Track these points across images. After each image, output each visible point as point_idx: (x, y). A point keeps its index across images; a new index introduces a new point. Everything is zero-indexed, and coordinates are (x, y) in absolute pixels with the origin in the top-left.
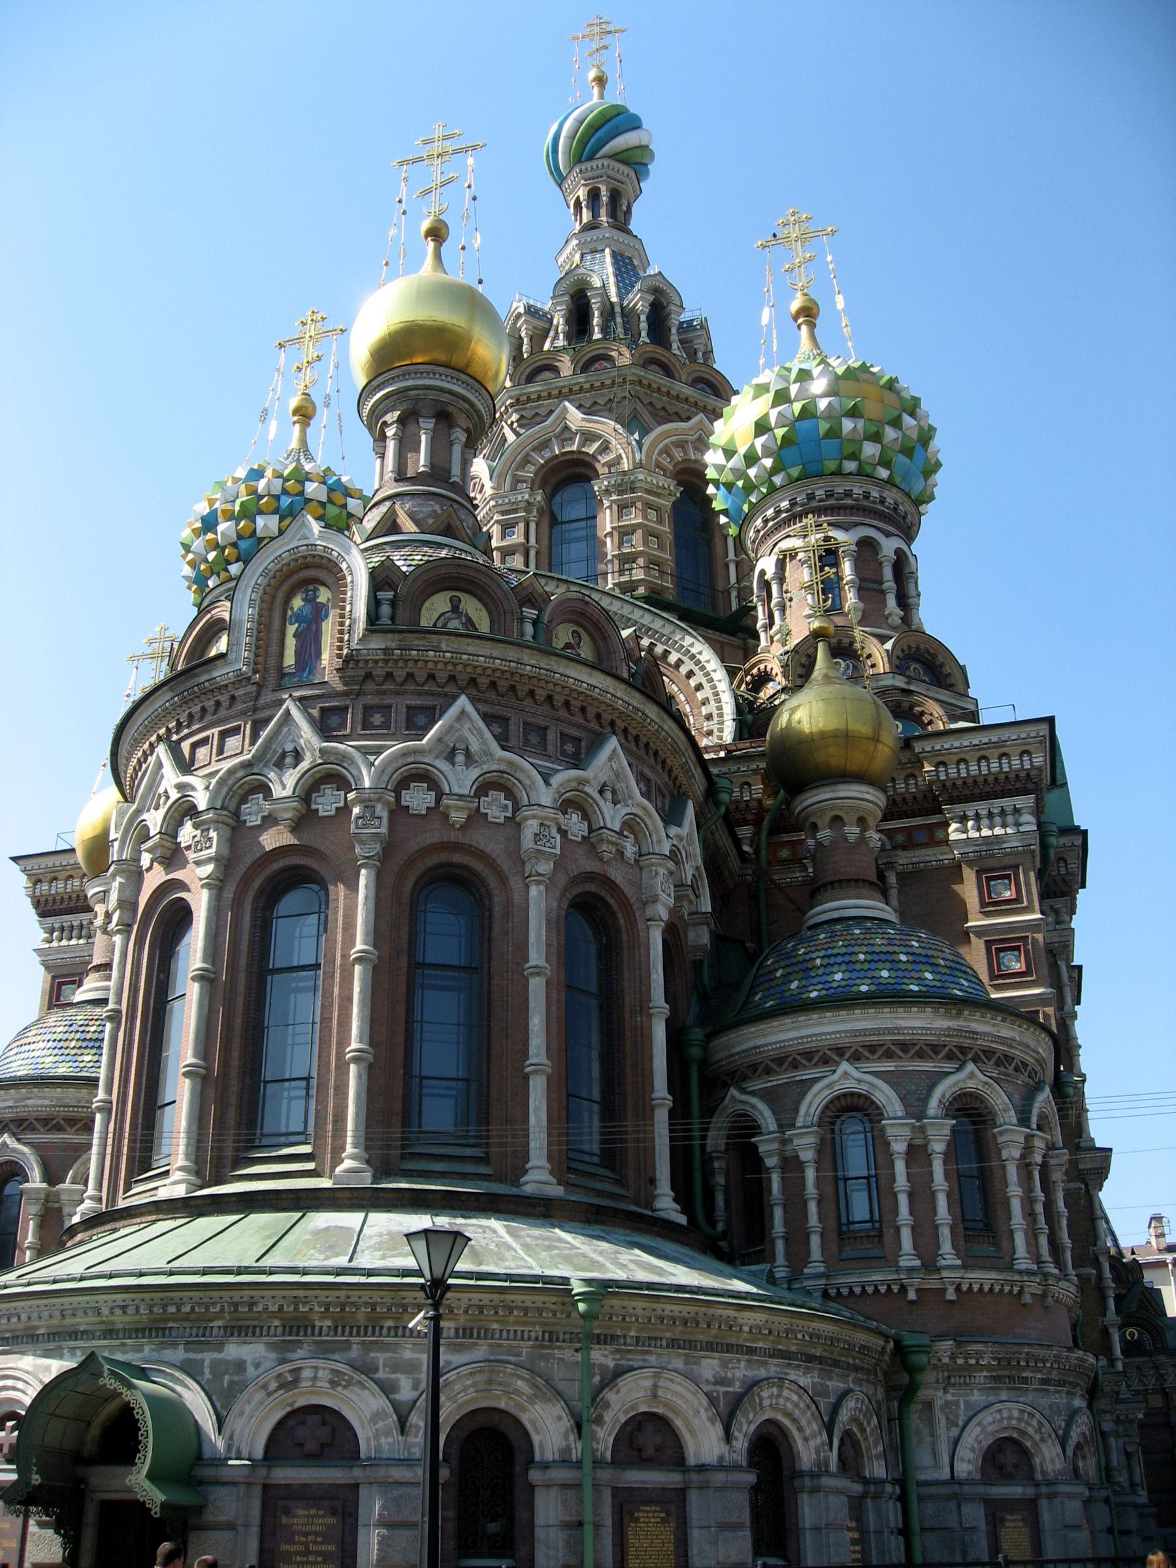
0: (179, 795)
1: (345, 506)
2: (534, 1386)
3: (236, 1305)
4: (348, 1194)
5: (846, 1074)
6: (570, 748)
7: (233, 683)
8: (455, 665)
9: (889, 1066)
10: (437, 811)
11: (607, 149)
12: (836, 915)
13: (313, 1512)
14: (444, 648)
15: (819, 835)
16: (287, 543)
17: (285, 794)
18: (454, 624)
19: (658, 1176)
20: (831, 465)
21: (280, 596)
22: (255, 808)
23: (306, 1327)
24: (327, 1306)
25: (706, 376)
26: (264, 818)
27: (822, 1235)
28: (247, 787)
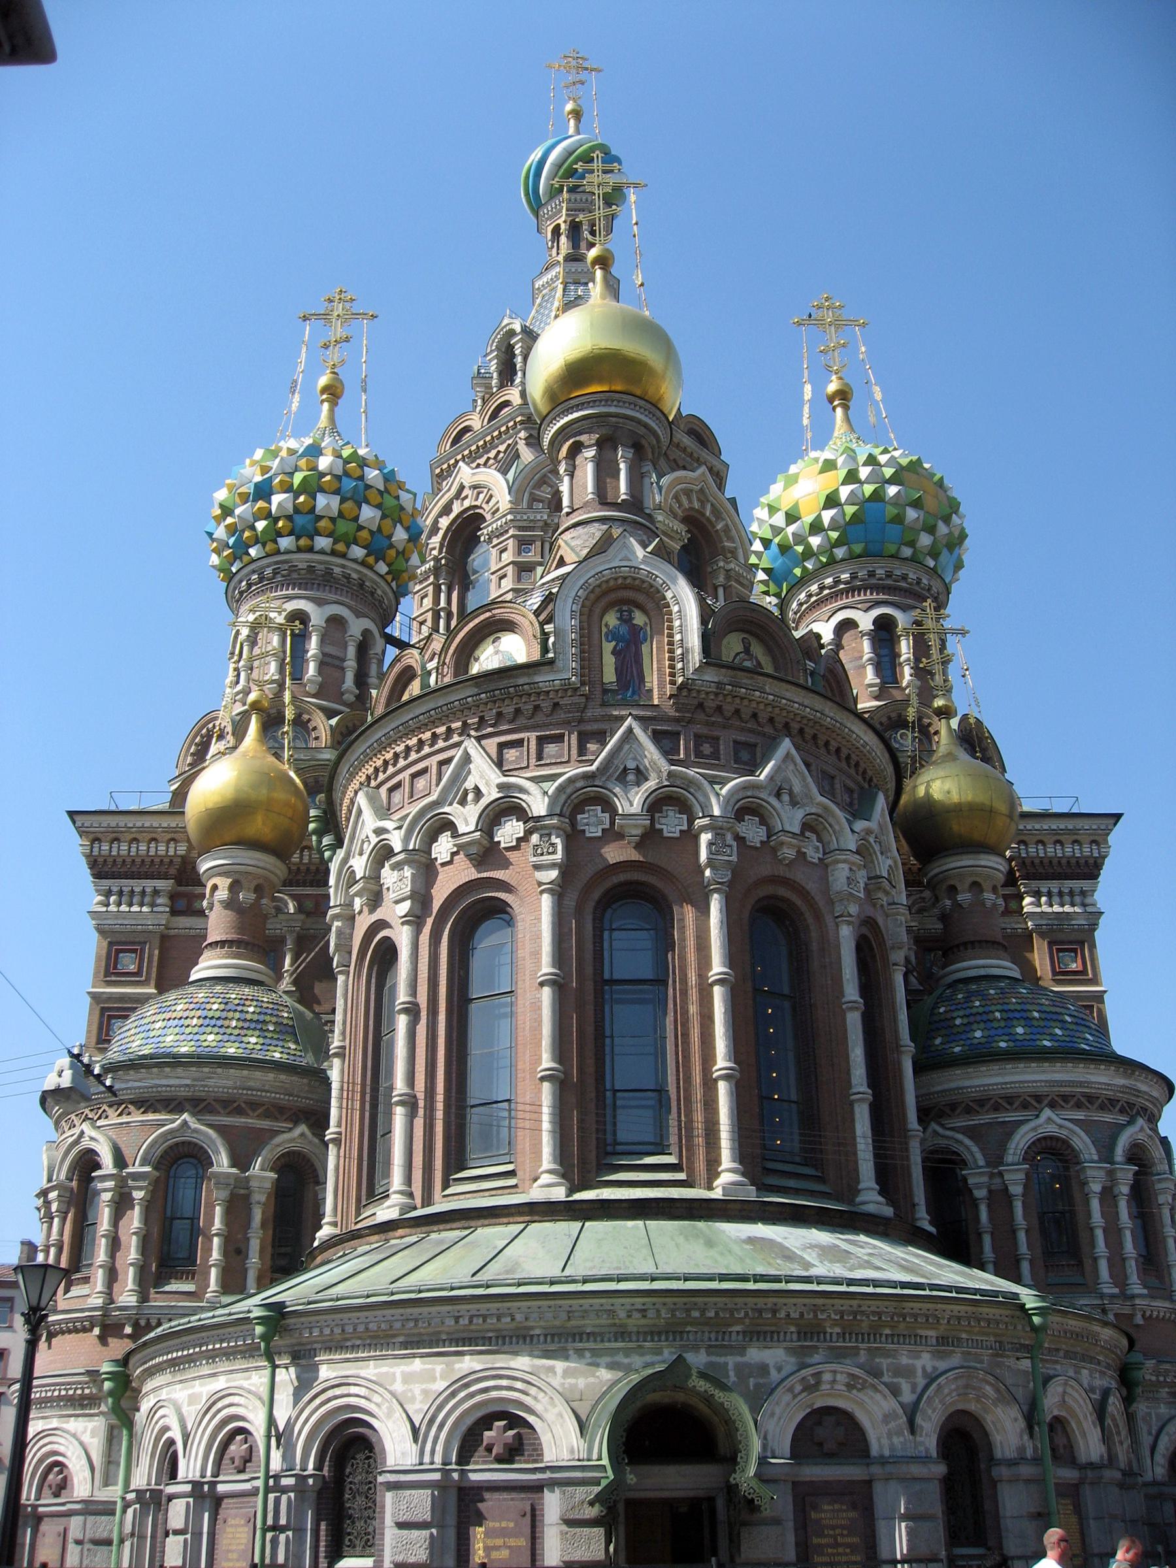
0: (501, 795)
1: (397, 498)
2: (998, 1391)
3: (760, 1311)
4: (738, 1206)
5: (1049, 1119)
6: (848, 800)
7: (557, 691)
9: (1080, 1115)
10: (769, 847)
12: (982, 972)
13: (837, 1506)
14: (768, 690)
15: (960, 898)
16: (609, 561)
18: (747, 664)
19: (916, 1200)
20: (891, 549)
21: (598, 610)
22: (593, 820)
23: (818, 1333)
24: (842, 1314)
27: (1031, 1262)
28: (582, 797)
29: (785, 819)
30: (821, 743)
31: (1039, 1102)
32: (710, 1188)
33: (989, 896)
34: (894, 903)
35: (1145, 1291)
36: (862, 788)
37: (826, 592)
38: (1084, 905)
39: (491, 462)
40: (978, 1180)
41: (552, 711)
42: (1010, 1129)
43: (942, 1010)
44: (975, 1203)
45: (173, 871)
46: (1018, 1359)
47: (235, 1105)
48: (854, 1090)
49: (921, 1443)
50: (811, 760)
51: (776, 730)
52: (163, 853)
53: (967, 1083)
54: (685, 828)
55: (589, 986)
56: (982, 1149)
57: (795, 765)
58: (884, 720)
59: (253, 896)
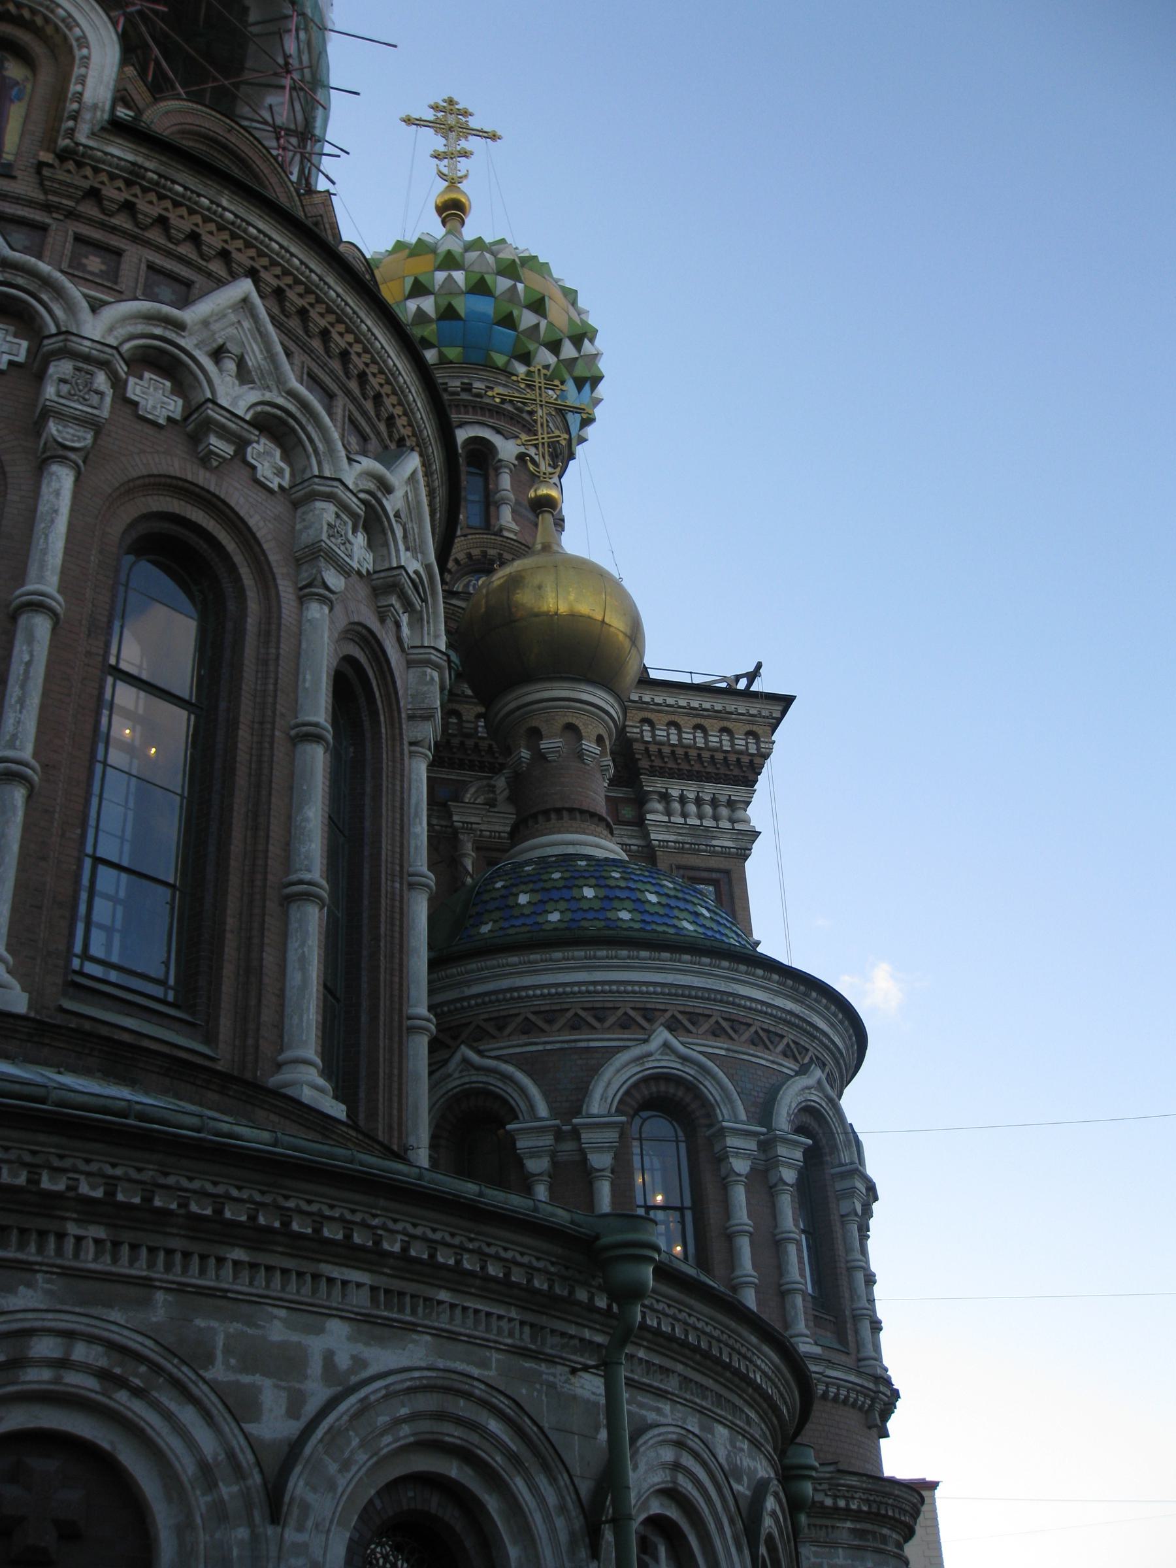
5: (666, 1045)
9: (719, 1047)
14: (225, 203)
15: (544, 745)
19: (412, 1141)
20: (500, 360)
23: (42, 1234)
31: (648, 1020)
33: (589, 745)
35: (817, 1350)
36: (386, 447)
38: (732, 821)
43: (499, 885)
46: (574, 1371)
48: (294, 877)
49: (301, 1549)
53: (527, 981)
54: (21, 358)
56: (546, 1095)
57: (254, 316)
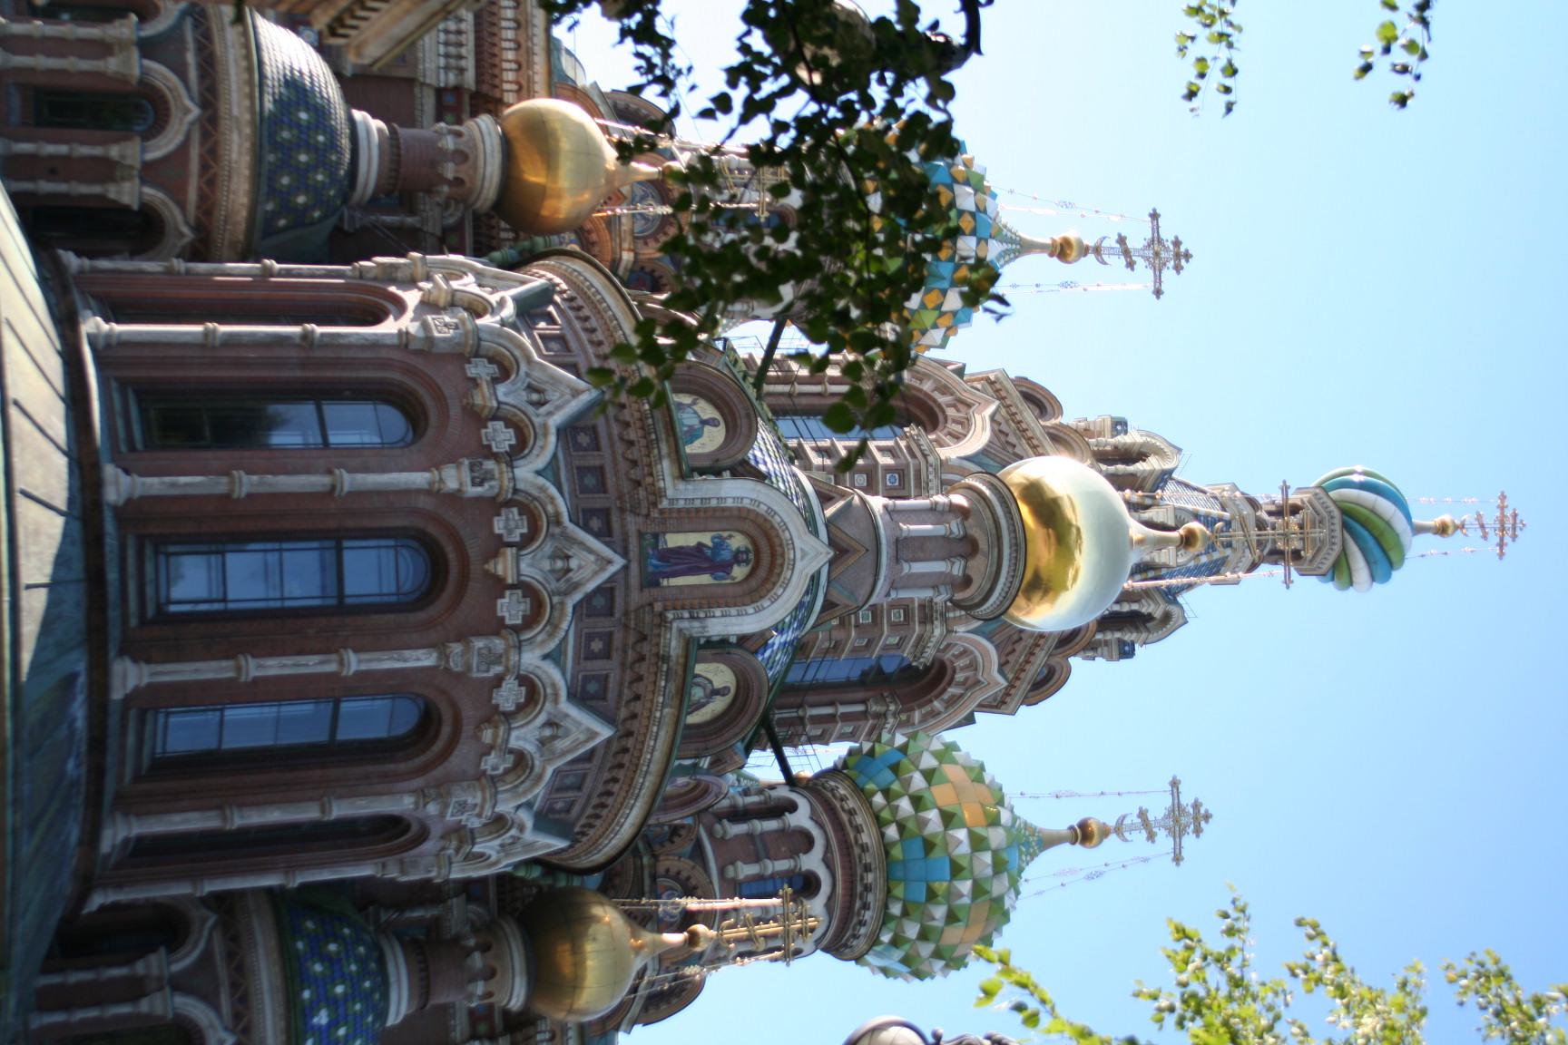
0: (536, 425)
1: (935, 326)
6: (559, 805)
7: (653, 485)
8: (649, 718)
10: (495, 716)
11: (1353, 549)
12: (393, 979)
14: (666, 710)
15: (477, 956)
16: (800, 537)
17: (523, 566)
18: (697, 693)
20: (899, 891)
21: (747, 526)
25: (1056, 676)
26: (500, 536)
29: (523, 730)
30: (615, 773)
32: (122, 652)
33: (480, 988)
34: (451, 863)
36: (573, 825)
37: (845, 817)
39: (1003, 438)
40: (153, 965)
41: (631, 480)
42: (211, 1000)
43: (347, 931)
44: (129, 962)
45: (485, 88)
47: (212, 163)
50: (597, 761)
51: (624, 721)
52: (505, 78)
53: (261, 951)
54: (508, 622)
55: (332, 524)
58: (693, 882)
59: (450, 175)
